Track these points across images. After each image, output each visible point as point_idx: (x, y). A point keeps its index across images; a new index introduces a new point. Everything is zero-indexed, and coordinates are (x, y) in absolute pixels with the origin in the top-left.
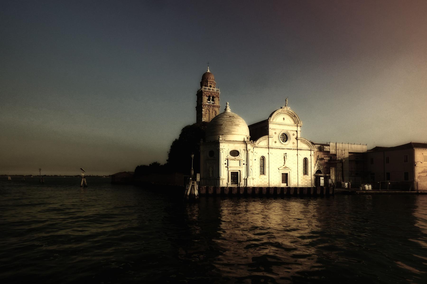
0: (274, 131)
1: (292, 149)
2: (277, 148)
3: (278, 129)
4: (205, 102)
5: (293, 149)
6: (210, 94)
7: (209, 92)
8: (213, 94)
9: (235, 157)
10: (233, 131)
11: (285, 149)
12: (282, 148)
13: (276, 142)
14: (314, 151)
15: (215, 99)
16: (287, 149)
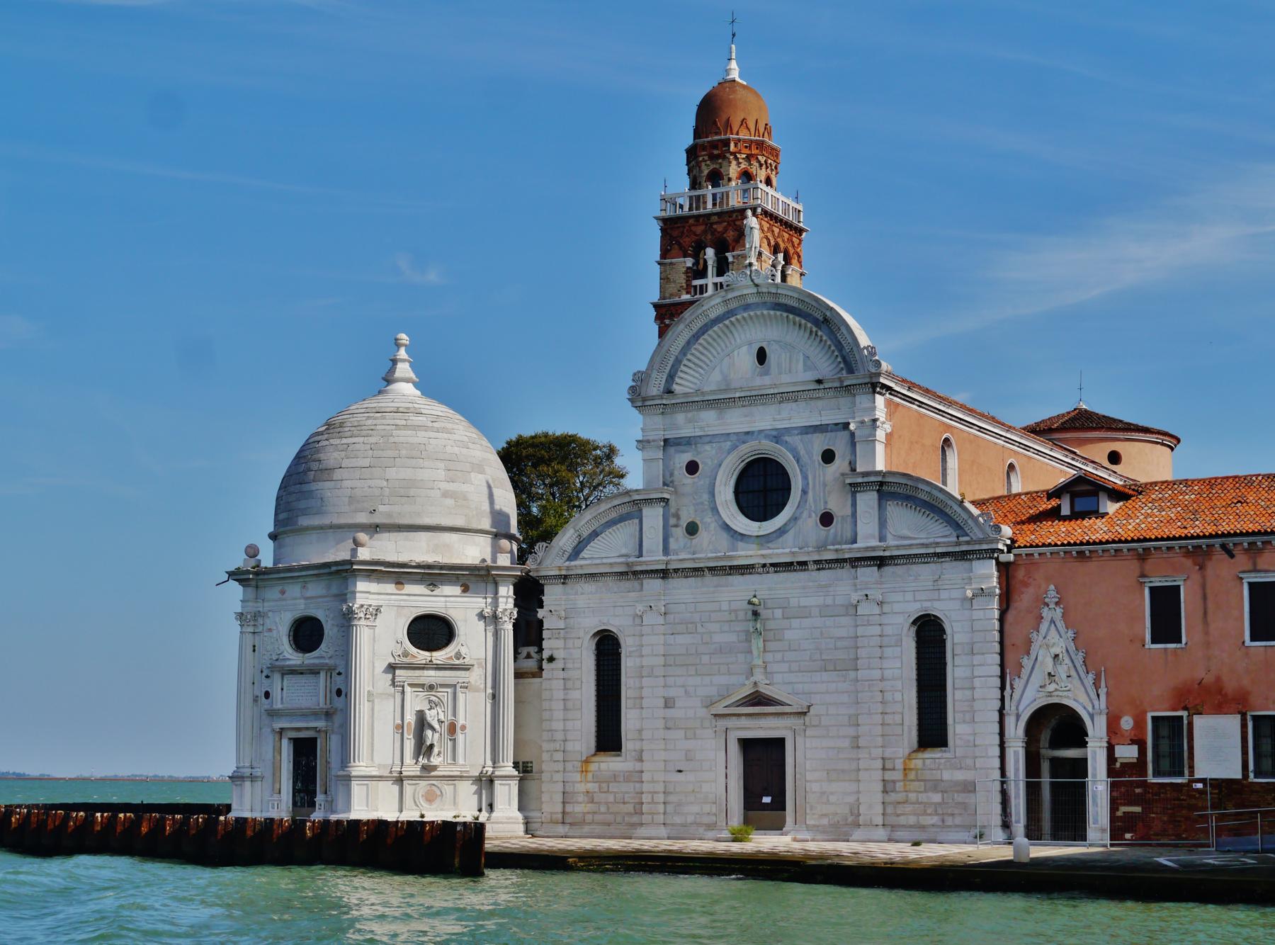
0: (677, 456)
1: (811, 566)
2: (695, 569)
3: (712, 439)
4: (675, 291)
5: (816, 562)
6: (699, 229)
7: (697, 217)
8: (719, 228)
9: (307, 655)
10: (305, 512)
11: (752, 567)
12: (731, 567)
13: (692, 529)
14: (1003, 558)
15: (730, 259)
16: (772, 565)
